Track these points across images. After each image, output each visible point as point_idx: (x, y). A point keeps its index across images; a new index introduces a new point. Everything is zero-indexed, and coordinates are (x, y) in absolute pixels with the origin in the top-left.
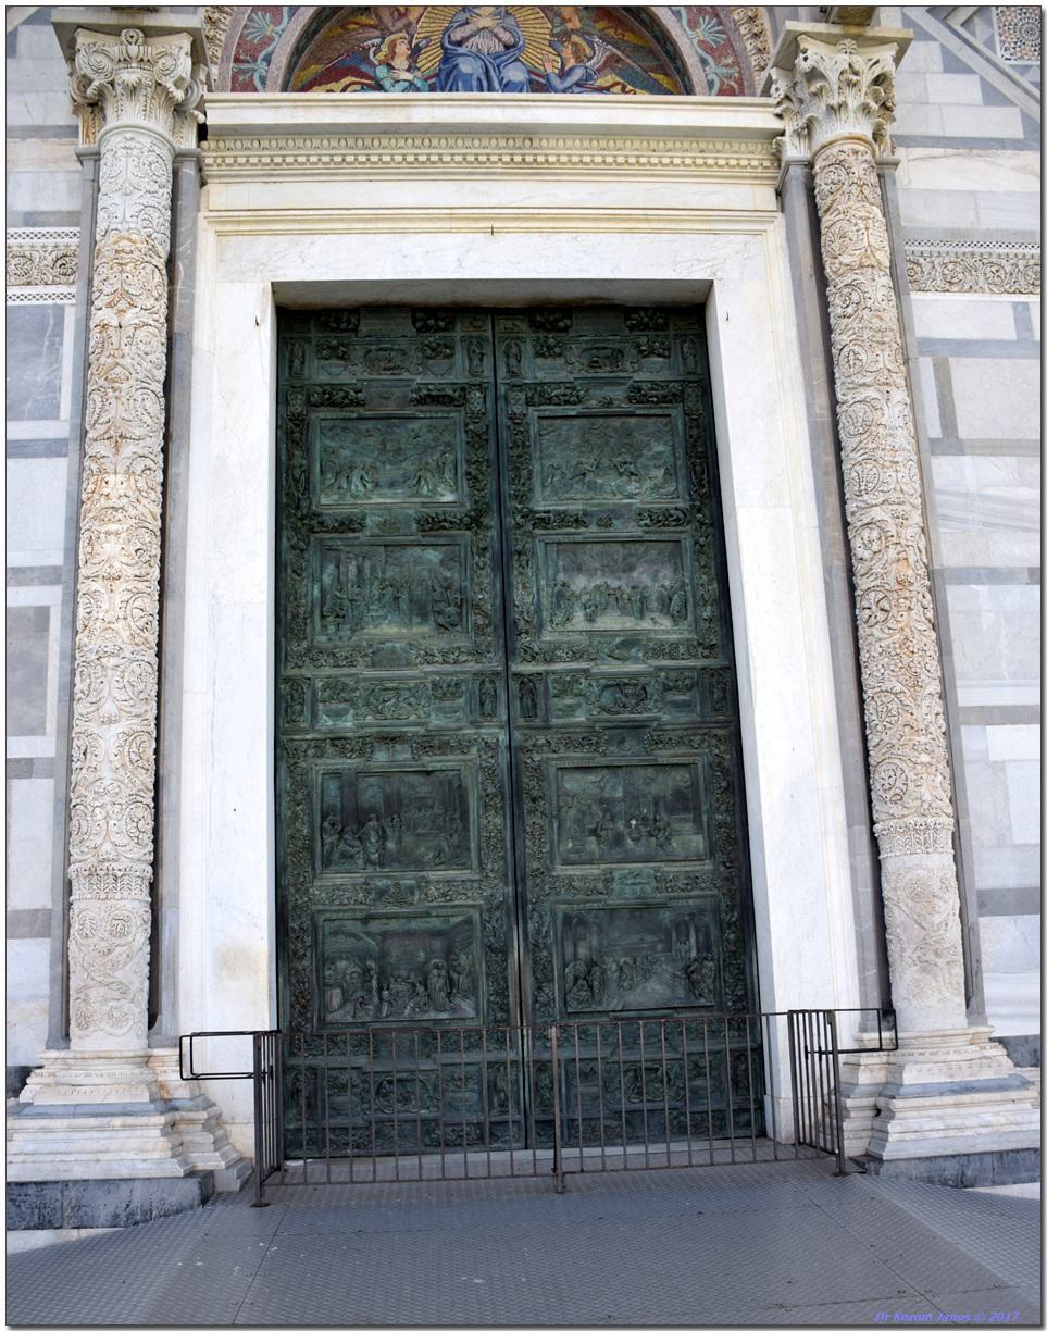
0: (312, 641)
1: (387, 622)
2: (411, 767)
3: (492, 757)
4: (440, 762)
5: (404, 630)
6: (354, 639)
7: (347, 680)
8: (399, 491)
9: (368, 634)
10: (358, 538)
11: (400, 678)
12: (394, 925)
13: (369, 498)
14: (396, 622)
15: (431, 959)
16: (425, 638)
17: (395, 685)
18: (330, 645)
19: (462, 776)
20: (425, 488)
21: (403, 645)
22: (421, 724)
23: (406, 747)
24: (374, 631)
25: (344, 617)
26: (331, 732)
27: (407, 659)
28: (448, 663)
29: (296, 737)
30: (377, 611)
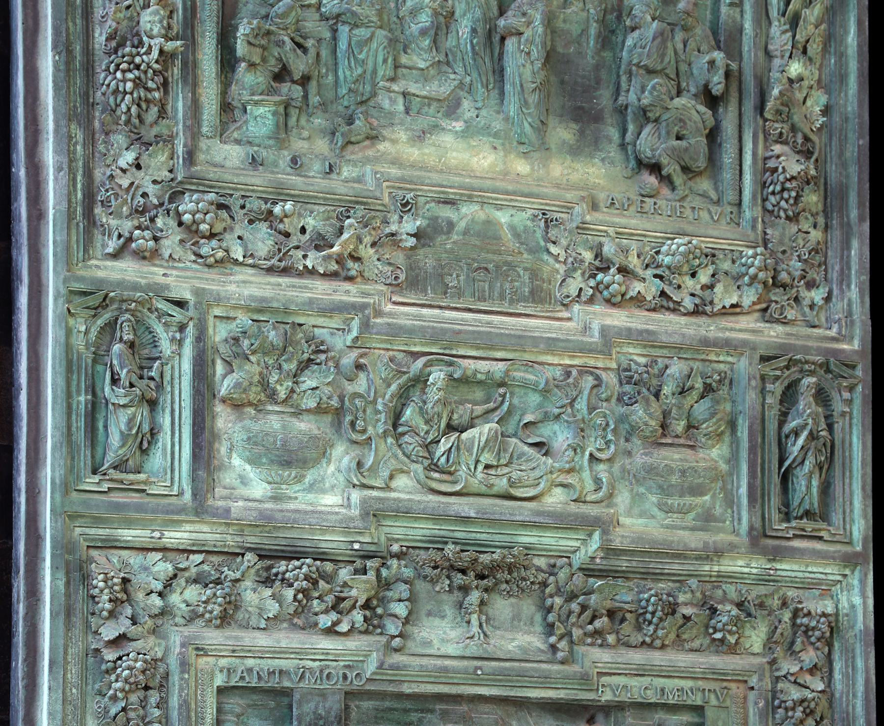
0: (190, 157)
1: (459, 126)
2: (545, 681)
3: (813, 670)
4: (640, 672)
5: (522, 167)
6: (347, 172)
9: (396, 162)
11: (520, 341)
14: (486, 130)
16: (594, 206)
17: (498, 368)
18: (258, 180)
21: (522, 219)
22: (588, 524)
23: (528, 607)
24: (413, 153)
25: (305, 81)
26: (265, 522)
27: (534, 274)
28: (675, 308)
29: (128, 534)
30: (424, 76)
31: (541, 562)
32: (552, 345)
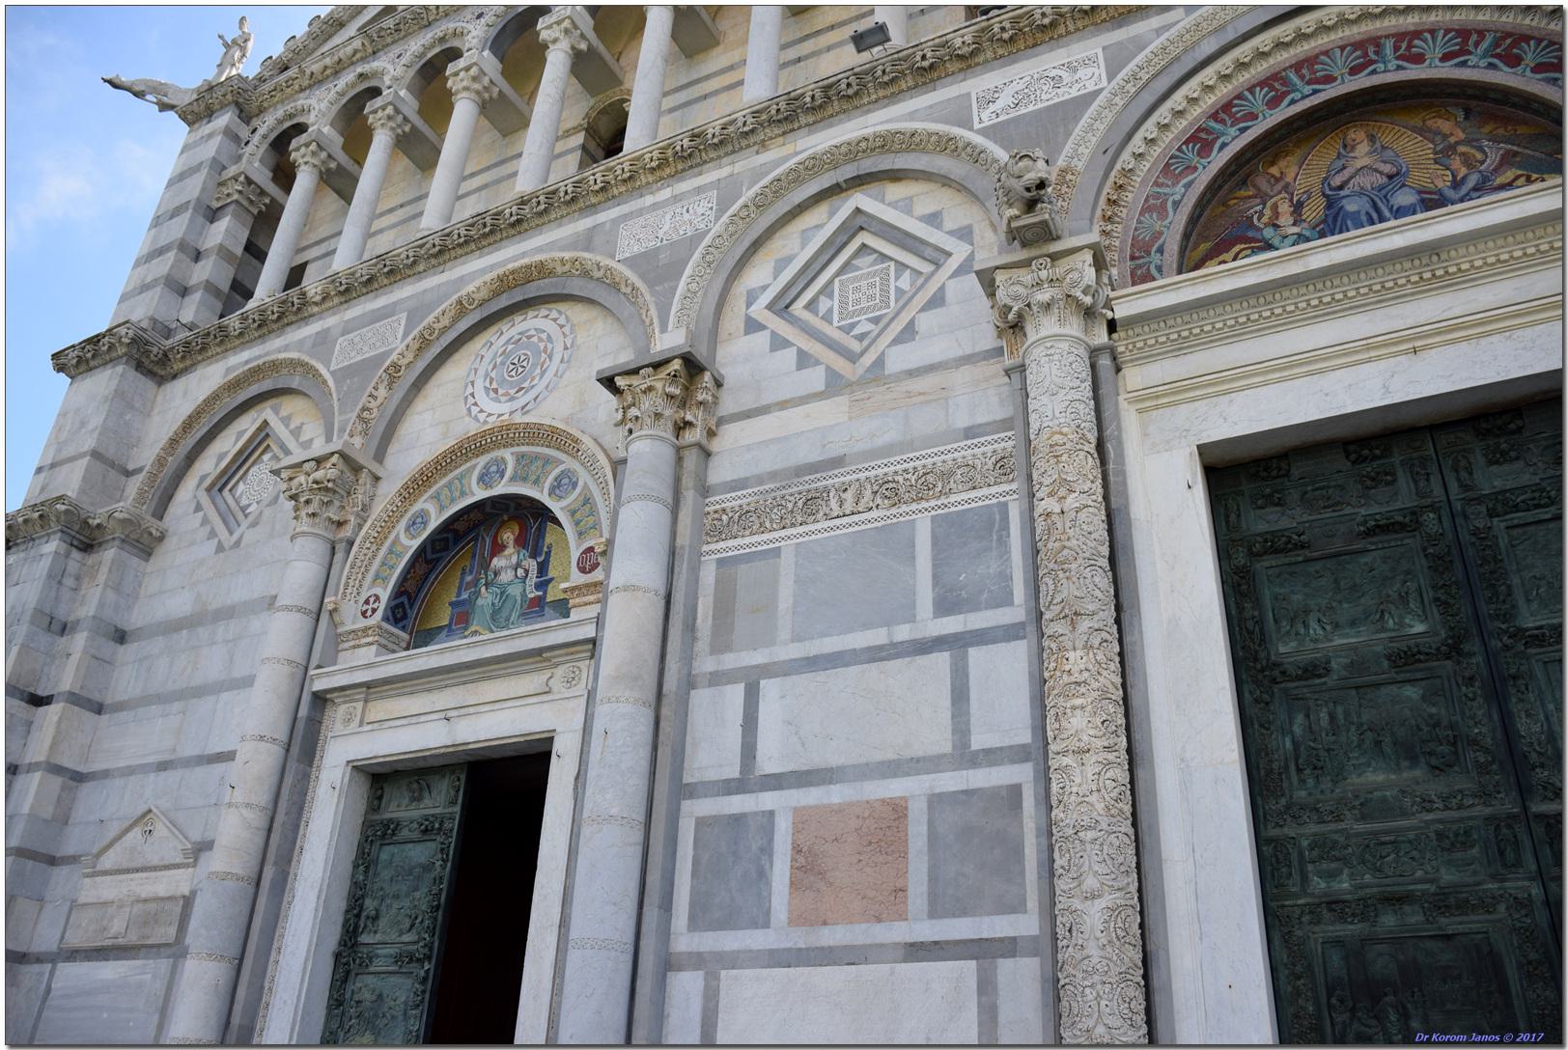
2: (1426, 930)
5: (1393, 777)
7: (1336, 837)
8: (1361, 629)
10: (1325, 683)
13: (1331, 641)
19: (1492, 940)
20: (1391, 621)
27: (1401, 808)
28: (1450, 809)
30: (1357, 758)
31: (1419, 894)
32: (1409, 829)
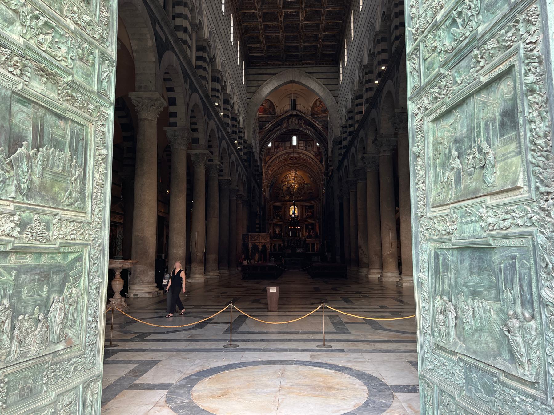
12: (29, 260)
15: (52, 292)
